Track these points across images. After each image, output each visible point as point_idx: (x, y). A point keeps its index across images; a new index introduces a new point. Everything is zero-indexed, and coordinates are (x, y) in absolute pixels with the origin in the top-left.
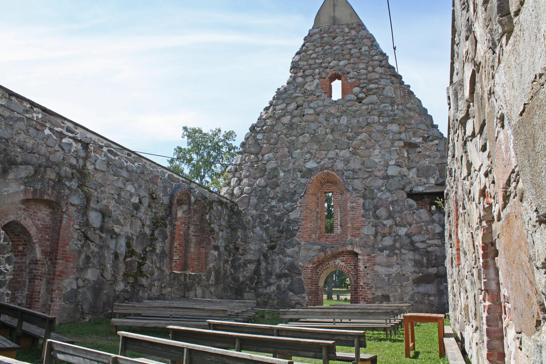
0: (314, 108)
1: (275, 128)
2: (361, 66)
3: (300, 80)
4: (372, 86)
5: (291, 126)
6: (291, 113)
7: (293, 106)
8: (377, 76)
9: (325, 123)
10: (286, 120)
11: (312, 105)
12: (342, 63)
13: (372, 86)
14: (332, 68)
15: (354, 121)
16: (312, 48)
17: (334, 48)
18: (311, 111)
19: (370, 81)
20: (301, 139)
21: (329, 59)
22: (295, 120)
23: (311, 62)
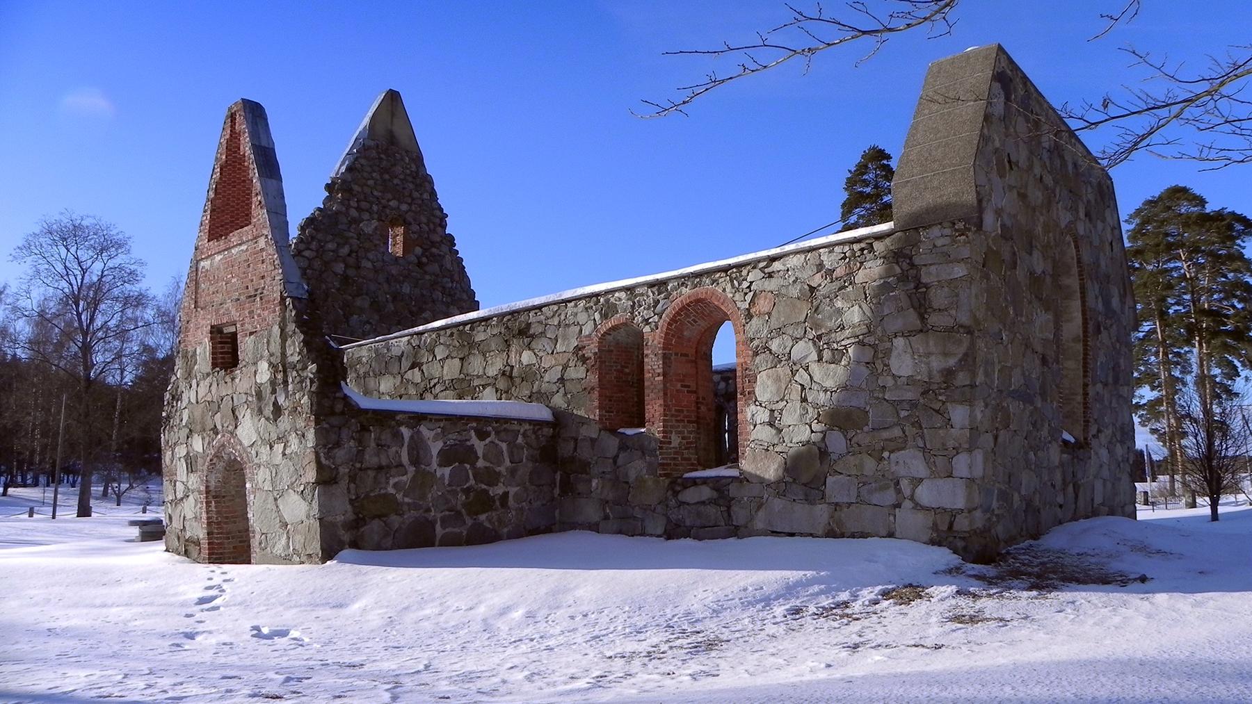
0: (373, 262)
1: (324, 275)
2: (424, 219)
3: (354, 213)
4: (434, 250)
5: (345, 279)
6: (344, 261)
7: (345, 251)
8: (438, 239)
9: (386, 286)
10: (339, 268)
11: (371, 256)
12: (404, 207)
13: (434, 250)
14: (392, 209)
15: (417, 291)
16: (369, 169)
17: (396, 181)
18: (369, 265)
19: (433, 244)
20: (358, 302)
21: (389, 196)
22: (351, 272)
23: (367, 190)
